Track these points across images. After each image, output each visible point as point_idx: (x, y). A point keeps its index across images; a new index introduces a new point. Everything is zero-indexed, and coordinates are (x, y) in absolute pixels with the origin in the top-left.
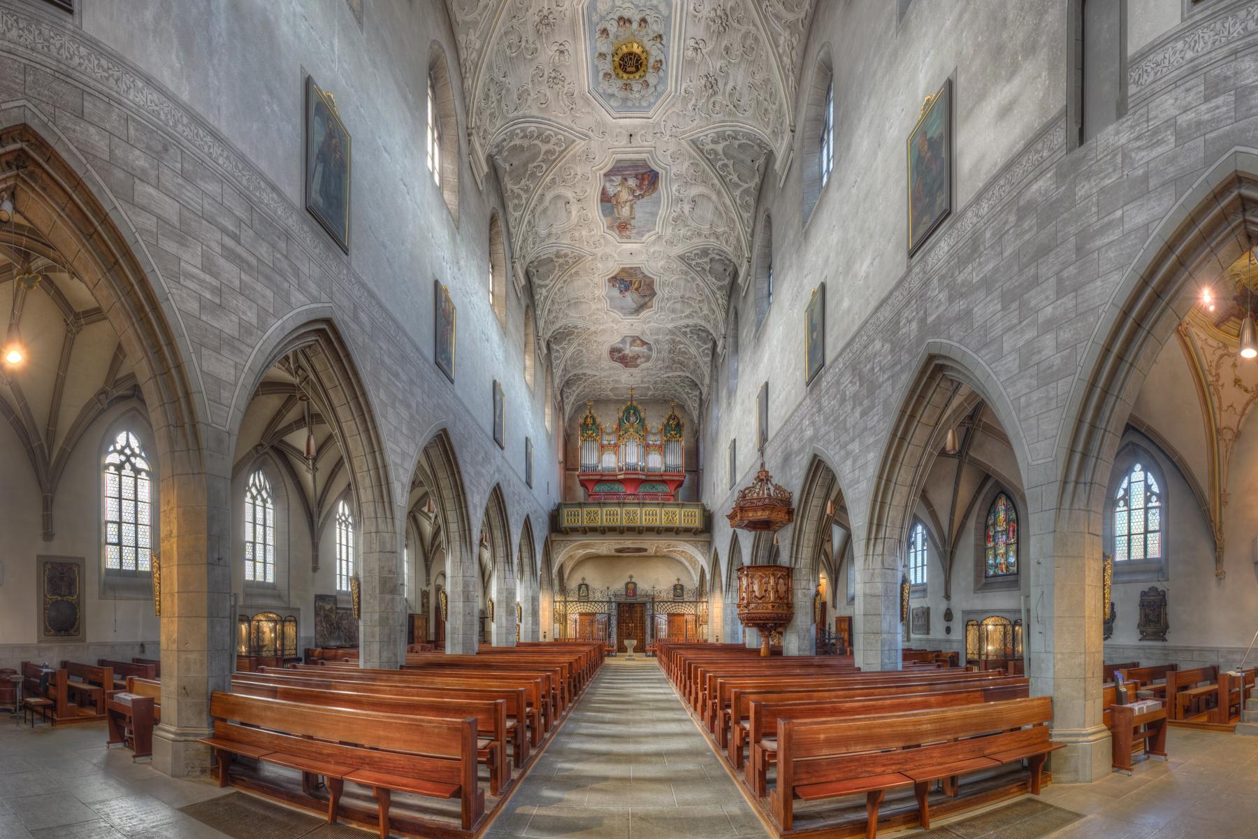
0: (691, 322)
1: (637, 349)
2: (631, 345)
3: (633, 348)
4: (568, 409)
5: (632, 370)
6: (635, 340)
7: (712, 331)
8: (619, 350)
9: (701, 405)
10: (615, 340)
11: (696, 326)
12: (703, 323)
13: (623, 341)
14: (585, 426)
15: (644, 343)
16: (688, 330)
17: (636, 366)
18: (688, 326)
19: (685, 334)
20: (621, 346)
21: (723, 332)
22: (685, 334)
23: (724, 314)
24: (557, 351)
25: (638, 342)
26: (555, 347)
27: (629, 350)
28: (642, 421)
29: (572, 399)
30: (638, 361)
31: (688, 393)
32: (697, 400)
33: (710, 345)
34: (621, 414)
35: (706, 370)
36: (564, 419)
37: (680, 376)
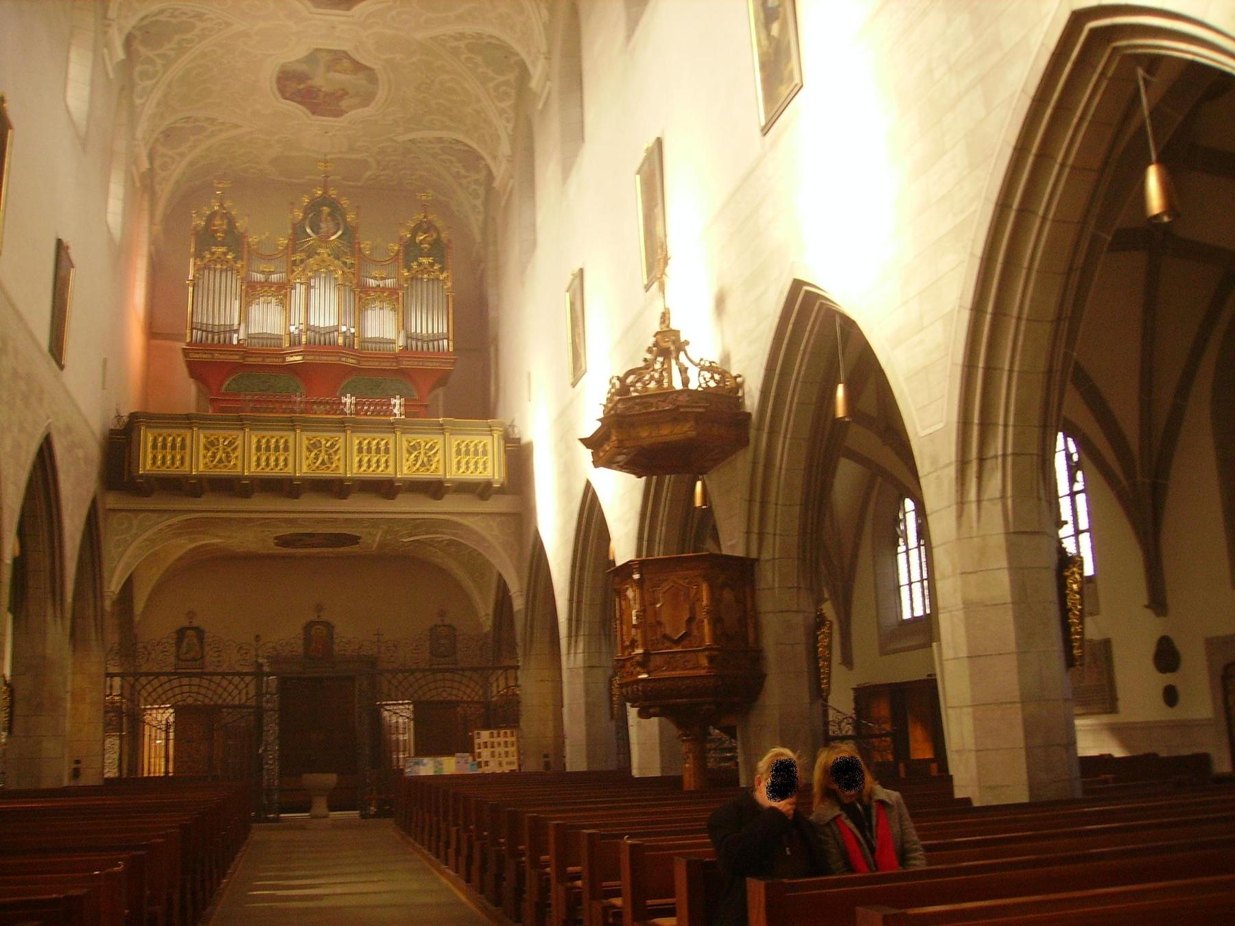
0: (468, 29)
1: (341, 77)
2: (329, 69)
3: (331, 75)
4: (165, 191)
5: (329, 121)
6: (338, 58)
7: (517, 47)
8: (301, 77)
9: (486, 203)
10: (294, 54)
11: (480, 36)
12: (496, 32)
13: (312, 57)
14: (205, 238)
15: (358, 67)
16: (462, 44)
17: (338, 113)
18: (462, 36)
19: (455, 52)
20: (304, 68)
21: (544, 48)
22: (455, 52)
23: (545, 13)
24: (150, 61)
25: (346, 63)
26: (144, 51)
27: (322, 80)
28: (350, 234)
29: (178, 170)
30: (344, 104)
31: (457, 176)
32: (482, 191)
33: (512, 76)
34: (299, 215)
35: (503, 128)
36: (152, 216)
37: (440, 140)
